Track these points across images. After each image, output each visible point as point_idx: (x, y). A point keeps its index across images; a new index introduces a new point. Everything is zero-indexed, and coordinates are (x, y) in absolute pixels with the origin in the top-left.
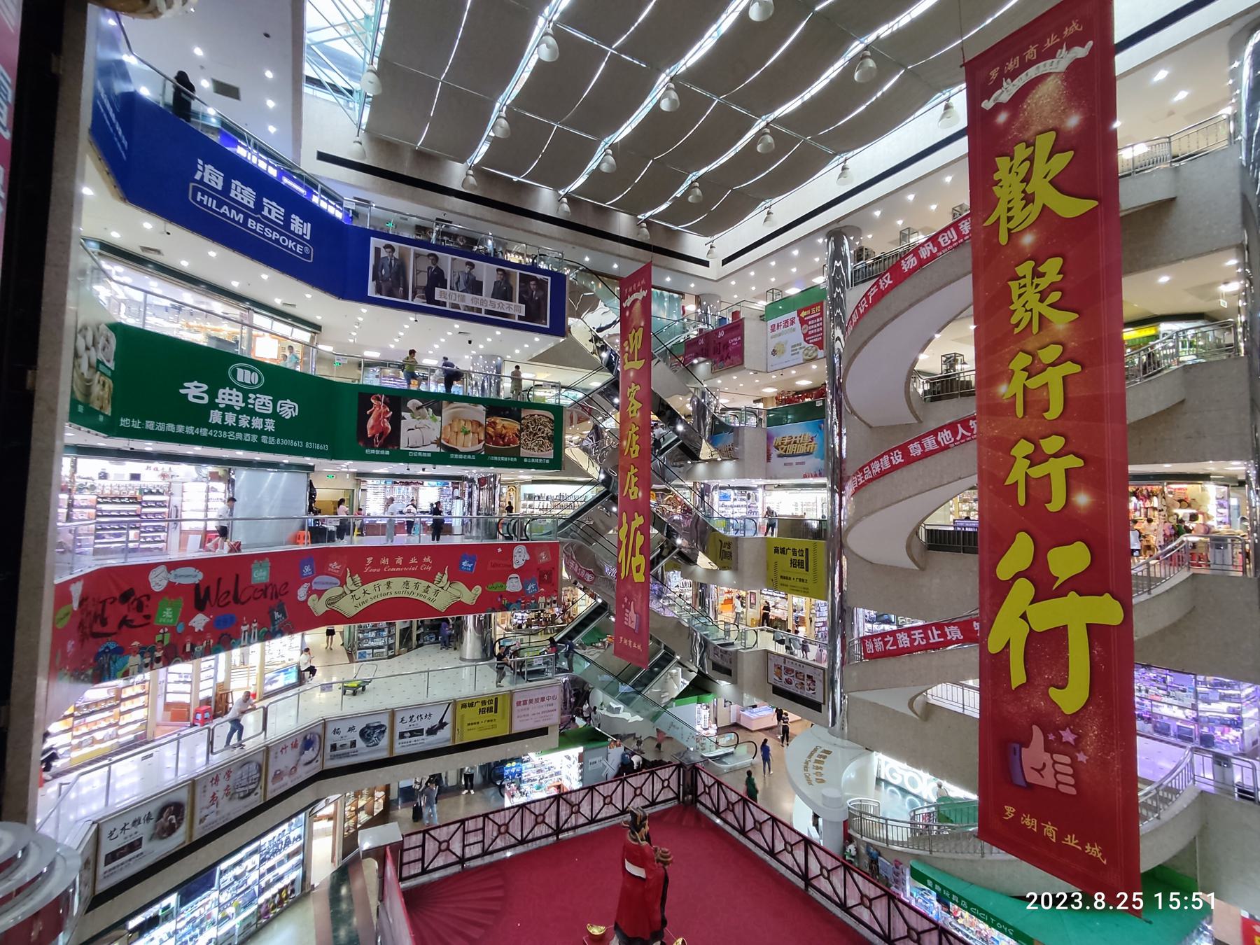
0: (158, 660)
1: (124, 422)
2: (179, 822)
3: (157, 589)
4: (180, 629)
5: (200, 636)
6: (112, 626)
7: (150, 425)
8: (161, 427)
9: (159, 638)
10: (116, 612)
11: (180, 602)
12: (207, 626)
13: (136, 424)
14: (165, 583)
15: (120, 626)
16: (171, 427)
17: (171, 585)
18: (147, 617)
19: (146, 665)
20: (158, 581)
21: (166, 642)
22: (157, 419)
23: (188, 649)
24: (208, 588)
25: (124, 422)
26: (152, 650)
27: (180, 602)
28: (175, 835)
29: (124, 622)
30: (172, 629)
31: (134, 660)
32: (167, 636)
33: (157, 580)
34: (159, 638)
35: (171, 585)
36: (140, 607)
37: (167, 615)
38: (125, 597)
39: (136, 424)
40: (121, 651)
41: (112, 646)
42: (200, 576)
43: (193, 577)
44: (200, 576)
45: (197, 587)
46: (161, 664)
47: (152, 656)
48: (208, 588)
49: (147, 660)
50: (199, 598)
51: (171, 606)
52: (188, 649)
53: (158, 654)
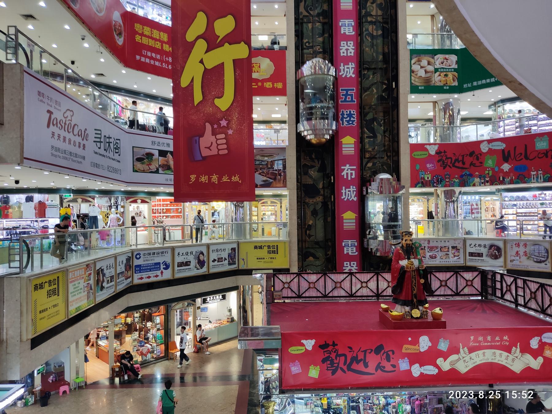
0: (487, 182)
1: (465, 86)
2: (500, 256)
3: (484, 151)
4: (497, 169)
5: (506, 174)
6: (467, 165)
7: (475, 84)
8: (480, 83)
9: (487, 172)
10: (468, 160)
11: (495, 157)
12: (510, 169)
13: (469, 85)
14: (487, 149)
15: (470, 166)
16: (484, 81)
17: (490, 149)
18: (481, 163)
19: (482, 183)
20: (484, 148)
21: (490, 174)
22: (477, 81)
23: (501, 179)
24: (509, 152)
25: (465, 86)
26: (485, 177)
27: (495, 157)
28: (497, 260)
29: (472, 164)
30: (493, 169)
31: (477, 180)
32: (491, 173)
33: (484, 147)
34: (487, 172)
35: (490, 149)
36: (478, 159)
37: (490, 162)
38: (471, 154)
39: (469, 85)
40: (471, 175)
41: (468, 173)
42: (504, 146)
43: (501, 146)
44: (504, 146)
45: (503, 151)
46: (489, 184)
47: (484, 179)
48: (509, 152)
49: (483, 181)
50: (505, 156)
51: (491, 159)
52: (501, 179)
53: (487, 179)
